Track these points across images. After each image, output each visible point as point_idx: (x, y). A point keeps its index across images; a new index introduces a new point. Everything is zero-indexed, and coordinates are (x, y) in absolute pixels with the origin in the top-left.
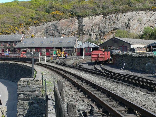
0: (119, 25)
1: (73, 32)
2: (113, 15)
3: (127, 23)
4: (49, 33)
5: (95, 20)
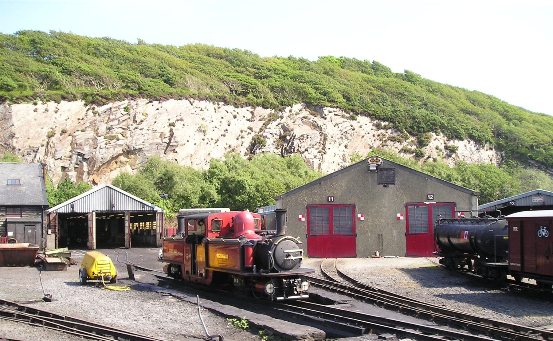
2: (120, 103)
3: (168, 135)
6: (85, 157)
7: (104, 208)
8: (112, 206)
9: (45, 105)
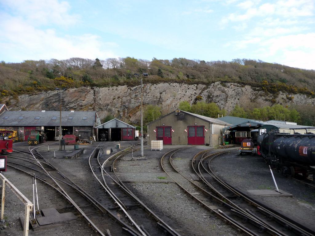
0: (149, 99)
1: (86, 106)
4: (51, 107)
5: (116, 91)
6: (126, 107)
7: (114, 126)
8: (117, 126)
9: (112, 88)
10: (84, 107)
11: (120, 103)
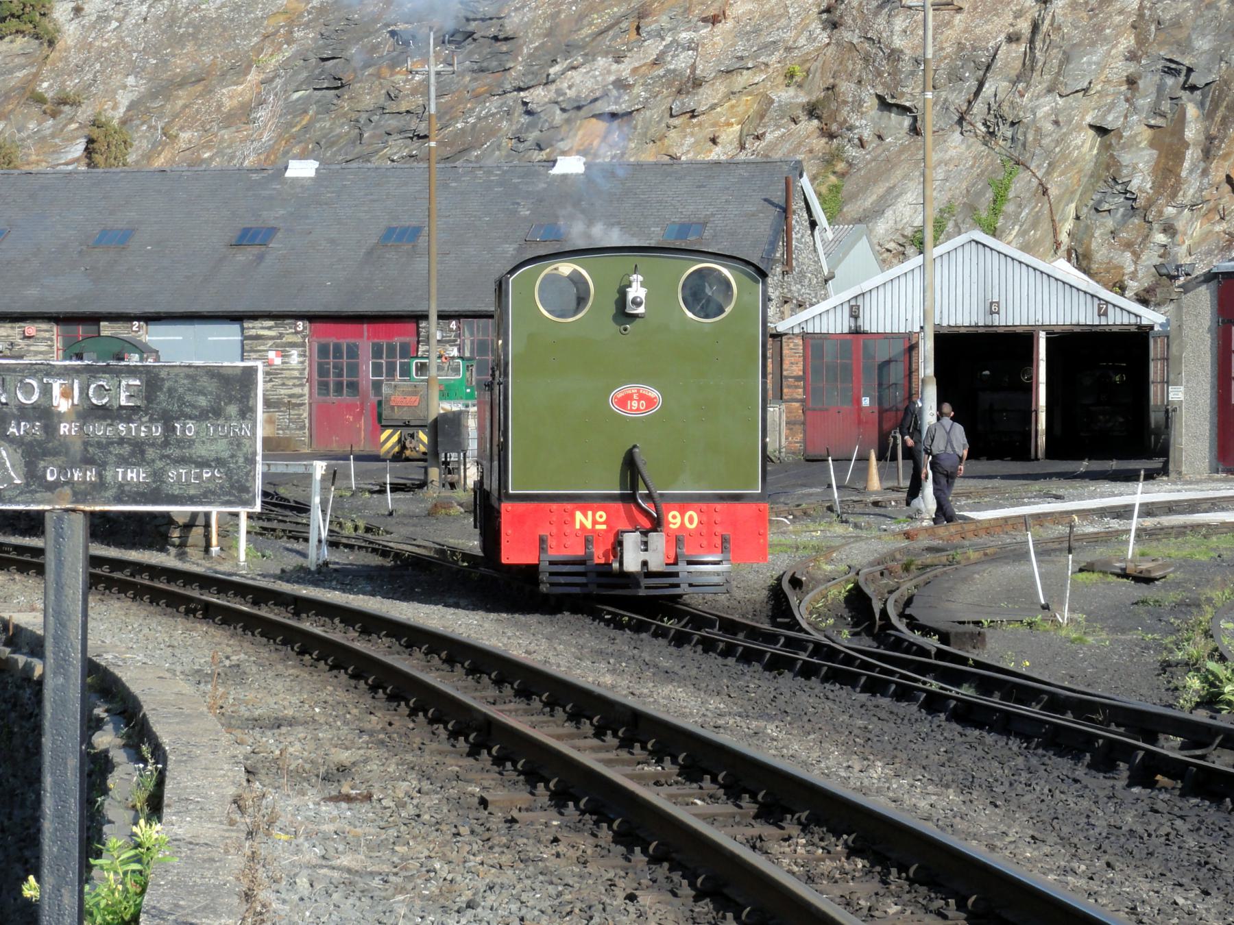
4: (368, 101)
10: (721, 88)
11: (1127, 41)
